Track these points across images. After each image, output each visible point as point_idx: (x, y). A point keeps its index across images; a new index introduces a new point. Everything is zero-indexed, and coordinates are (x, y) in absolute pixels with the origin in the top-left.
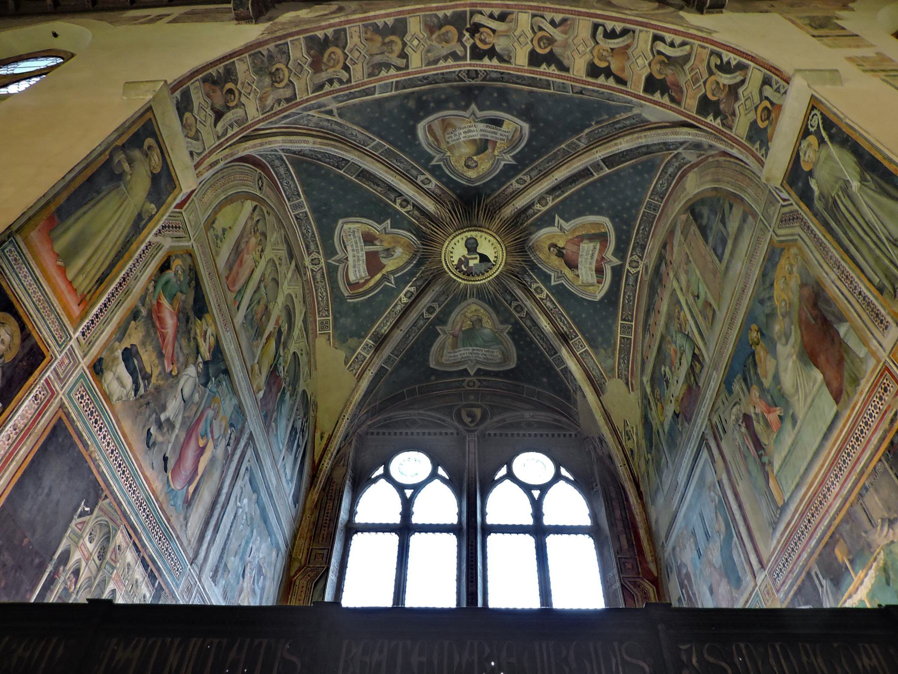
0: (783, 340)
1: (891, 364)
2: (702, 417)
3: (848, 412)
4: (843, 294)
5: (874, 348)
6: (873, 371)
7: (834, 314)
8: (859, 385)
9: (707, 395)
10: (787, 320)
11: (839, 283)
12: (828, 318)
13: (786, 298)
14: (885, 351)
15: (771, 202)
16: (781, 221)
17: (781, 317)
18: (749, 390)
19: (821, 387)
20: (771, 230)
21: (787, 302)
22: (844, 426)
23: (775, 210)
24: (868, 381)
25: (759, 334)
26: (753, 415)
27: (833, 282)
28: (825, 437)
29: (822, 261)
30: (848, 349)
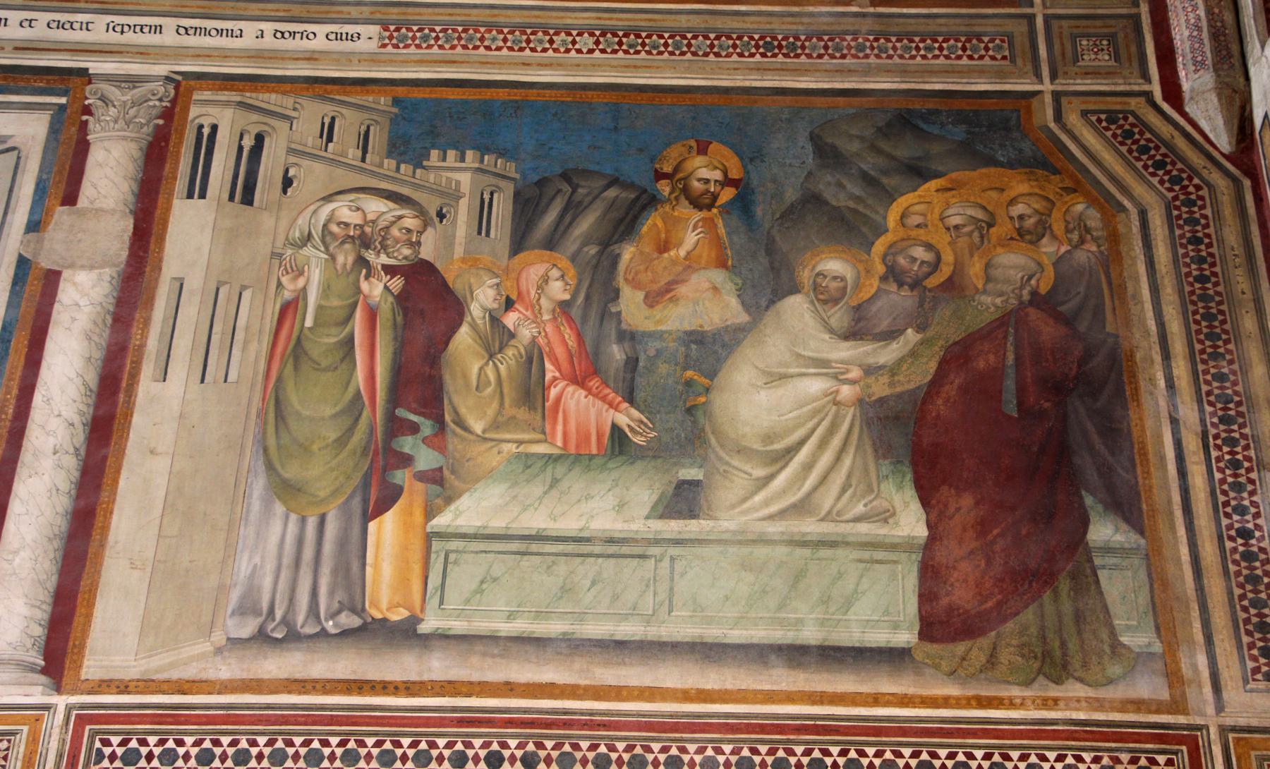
0: (839, 316)
1: (1217, 750)
2: (130, 37)
3: (953, 690)
4: (1182, 473)
5: (1186, 670)
6: (1139, 705)
7: (1106, 472)
8: (1058, 681)
9: (250, 28)
10: (902, 299)
11: (1192, 444)
12: (1077, 460)
13: (948, 257)
14: (1220, 708)
15: (1112, 38)
16: (1112, 117)
17: (880, 269)
18: (518, 245)
19: (893, 547)
20: (1047, 86)
21: (945, 271)
22: (904, 701)
23: (1109, 74)
24: (1099, 704)
25: (727, 194)
26: (475, 310)
27: (1174, 422)
28: (796, 654)
29: (1178, 346)
30: (1086, 580)
